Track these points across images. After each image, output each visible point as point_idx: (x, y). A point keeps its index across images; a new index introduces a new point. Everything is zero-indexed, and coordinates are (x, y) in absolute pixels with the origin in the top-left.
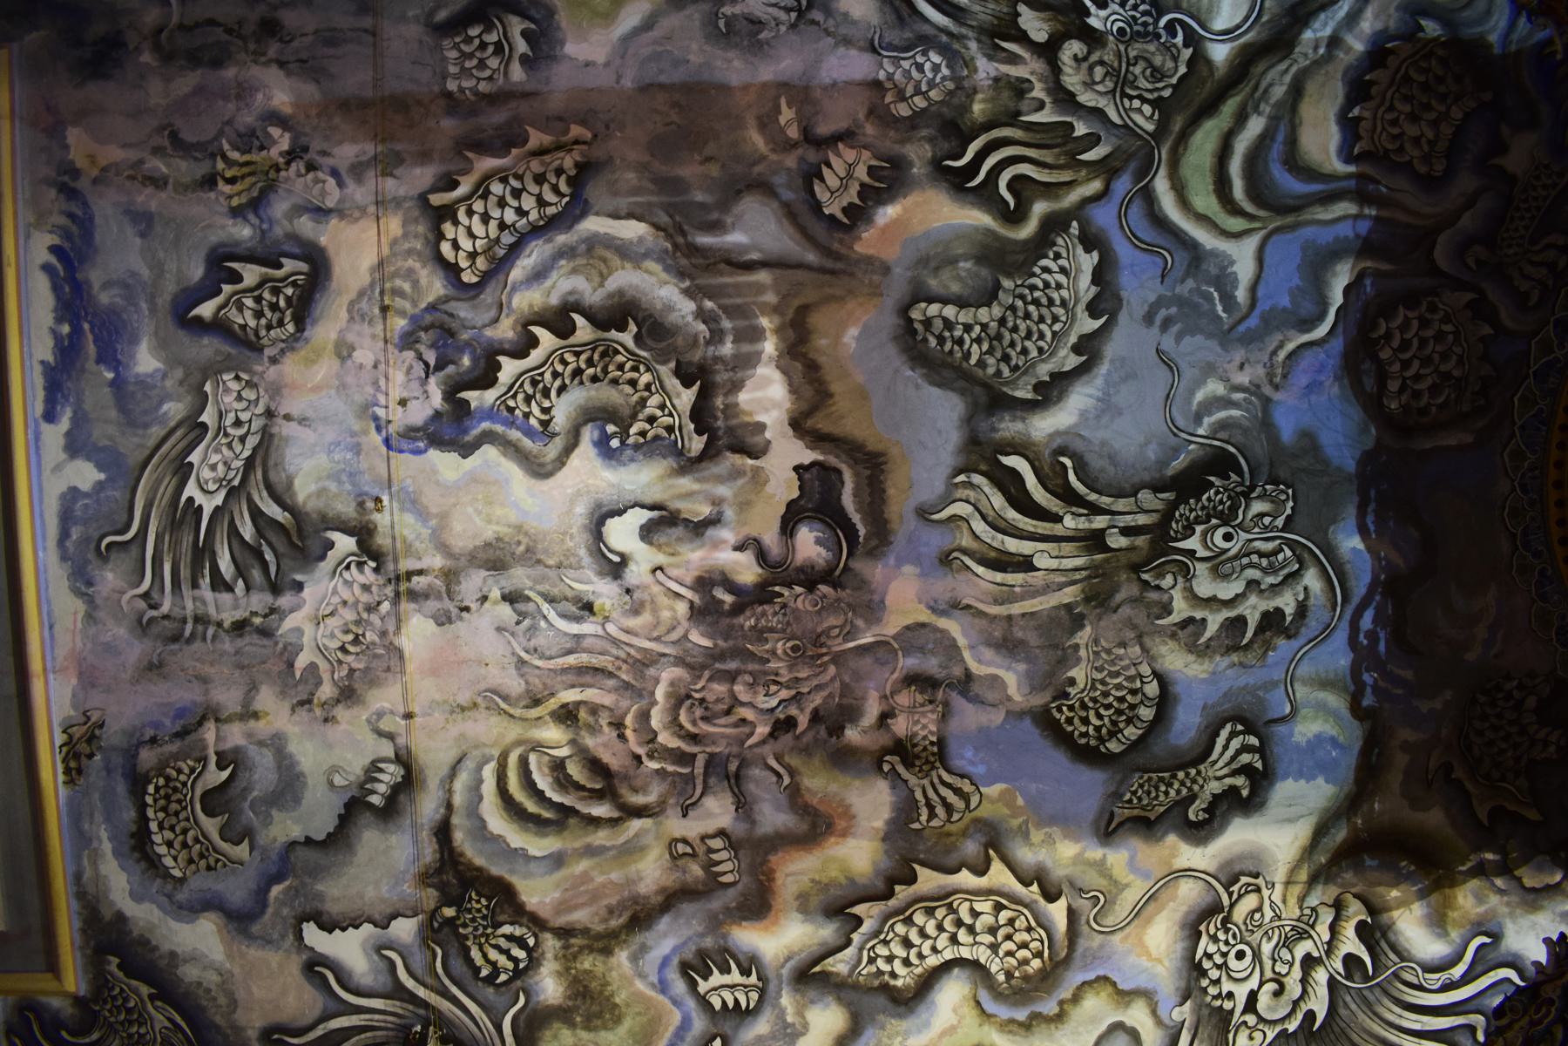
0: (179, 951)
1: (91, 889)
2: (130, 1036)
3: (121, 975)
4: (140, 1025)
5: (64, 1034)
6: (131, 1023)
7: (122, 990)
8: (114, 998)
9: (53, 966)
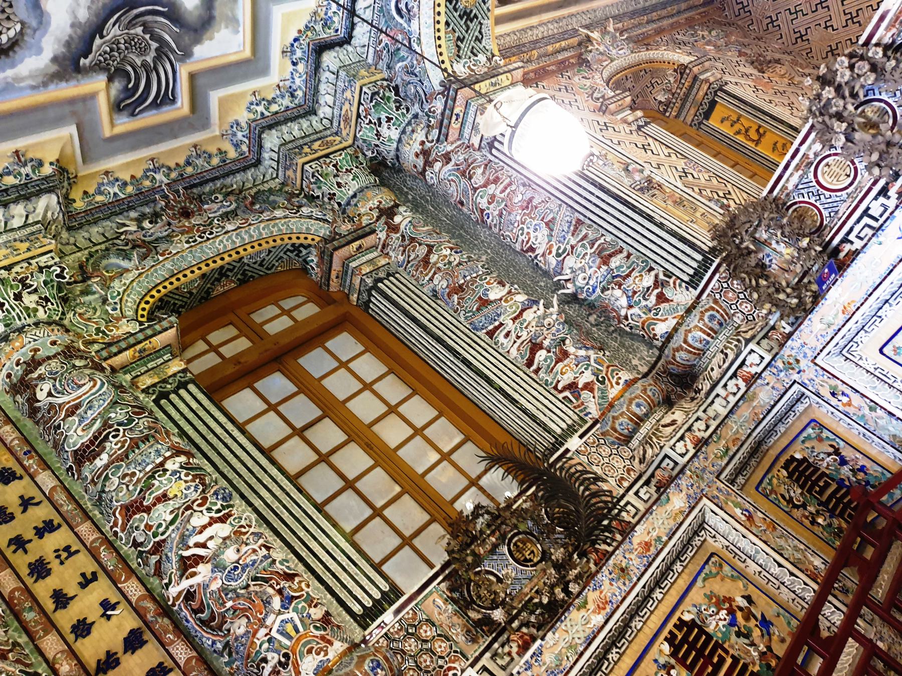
0: (69, 22)
1: (40, 79)
2: (127, 48)
3: (91, 57)
4: (119, 43)
5: (130, 86)
6: (119, 49)
7: (100, 55)
8: (105, 59)
9: (93, 96)
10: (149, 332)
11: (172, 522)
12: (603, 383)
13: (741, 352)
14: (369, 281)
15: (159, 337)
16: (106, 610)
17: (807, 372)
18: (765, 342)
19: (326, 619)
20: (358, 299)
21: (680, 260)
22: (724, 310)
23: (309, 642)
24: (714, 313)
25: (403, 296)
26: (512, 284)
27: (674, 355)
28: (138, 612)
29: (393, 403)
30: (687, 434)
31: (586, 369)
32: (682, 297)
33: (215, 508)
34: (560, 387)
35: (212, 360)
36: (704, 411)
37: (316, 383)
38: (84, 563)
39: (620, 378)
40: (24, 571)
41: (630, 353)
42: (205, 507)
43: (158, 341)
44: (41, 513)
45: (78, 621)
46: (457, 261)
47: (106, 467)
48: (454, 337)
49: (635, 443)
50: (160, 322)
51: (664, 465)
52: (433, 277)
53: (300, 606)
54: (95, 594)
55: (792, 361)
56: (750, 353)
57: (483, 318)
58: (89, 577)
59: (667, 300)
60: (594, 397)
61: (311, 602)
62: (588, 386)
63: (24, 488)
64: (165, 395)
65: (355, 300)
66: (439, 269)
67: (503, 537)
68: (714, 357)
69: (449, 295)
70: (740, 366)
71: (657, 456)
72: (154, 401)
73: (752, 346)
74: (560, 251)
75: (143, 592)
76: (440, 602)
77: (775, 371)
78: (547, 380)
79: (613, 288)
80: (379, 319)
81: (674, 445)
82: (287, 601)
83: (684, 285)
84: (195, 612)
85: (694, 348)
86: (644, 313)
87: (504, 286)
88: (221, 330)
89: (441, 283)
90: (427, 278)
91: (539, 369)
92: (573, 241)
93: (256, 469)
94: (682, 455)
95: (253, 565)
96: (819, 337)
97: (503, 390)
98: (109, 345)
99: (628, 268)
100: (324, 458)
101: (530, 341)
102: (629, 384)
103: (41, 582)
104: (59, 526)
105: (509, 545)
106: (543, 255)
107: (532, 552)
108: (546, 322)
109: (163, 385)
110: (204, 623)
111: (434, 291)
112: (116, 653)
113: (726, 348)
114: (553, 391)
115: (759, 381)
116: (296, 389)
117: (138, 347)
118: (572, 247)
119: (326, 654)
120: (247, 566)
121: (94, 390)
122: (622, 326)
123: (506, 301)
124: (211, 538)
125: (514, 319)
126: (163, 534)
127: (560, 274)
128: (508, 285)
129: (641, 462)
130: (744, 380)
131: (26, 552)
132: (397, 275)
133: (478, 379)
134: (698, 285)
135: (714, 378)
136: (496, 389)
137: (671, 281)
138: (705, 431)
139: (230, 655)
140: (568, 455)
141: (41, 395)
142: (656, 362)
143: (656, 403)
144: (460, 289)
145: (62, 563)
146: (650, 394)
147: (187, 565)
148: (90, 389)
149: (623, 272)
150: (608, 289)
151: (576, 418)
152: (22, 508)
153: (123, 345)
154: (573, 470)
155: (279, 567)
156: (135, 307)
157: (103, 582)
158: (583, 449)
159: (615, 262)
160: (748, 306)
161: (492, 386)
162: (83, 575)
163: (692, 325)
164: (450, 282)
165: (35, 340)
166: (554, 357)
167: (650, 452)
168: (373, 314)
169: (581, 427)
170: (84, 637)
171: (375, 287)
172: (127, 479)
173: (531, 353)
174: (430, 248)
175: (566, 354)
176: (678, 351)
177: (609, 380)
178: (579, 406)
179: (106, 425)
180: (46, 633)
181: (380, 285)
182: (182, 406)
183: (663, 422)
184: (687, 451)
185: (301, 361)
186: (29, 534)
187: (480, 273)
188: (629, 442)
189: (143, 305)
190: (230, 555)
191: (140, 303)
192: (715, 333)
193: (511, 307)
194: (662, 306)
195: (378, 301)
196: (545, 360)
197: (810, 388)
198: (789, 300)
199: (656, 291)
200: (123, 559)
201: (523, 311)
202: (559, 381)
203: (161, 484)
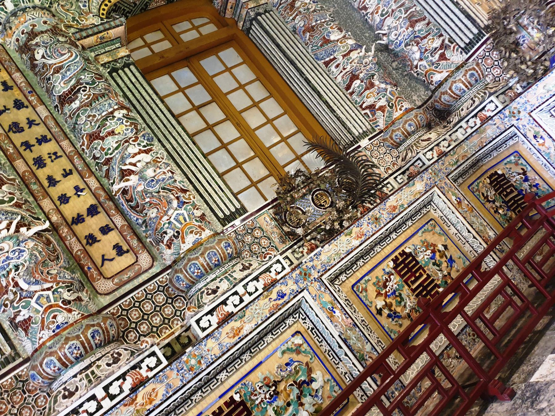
10: (107, 26)
11: (117, 148)
12: (391, 107)
13: (485, 101)
14: (252, 14)
15: (114, 30)
16: (77, 191)
17: (523, 120)
18: (501, 97)
19: (203, 217)
20: (243, 26)
21: (462, 32)
22: (481, 71)
23: (191, 227)
24: (474, 72)
25: (273, 28)
26: (347, 31)
27: (441, 97)
29: (257, 100)
30: (436, 148)
31: (383, 97)
32: (457, 58)
33: (142, 144)
34: (363, 107)
35: (146, 52)
36: (450, 135)
37: (210, 78)
38: (64, 163)
39: (403, 106)
40: (31, 162)
41: (413, 91)
42: (136, 143)
43: (113, 33)
44: (39, 131)
45: (62, 194)
46: (313, 9)
47: (78, 109)
48: (302, 62)
49: (402, 148)
50: (114, 20)
51: (416, 164)
52: (295, 17)
53: (188, 208)
54: (71, 182)
55: (515, 111)
56: (490, 102)
57: (324, 52)
58: (68, 172)
59: (446, 59)
60: (384, 116)
61: (195, 207)
62: (382, 109)
63: (29, 113)
64: (115, 70)
65: (241, 26)
66: (300, 12)
67: (310, 190)
68: (465, 102)
69: (304, 32)
70: (481, 110)
71: (414, 158)
72: (108, 72)
73: (492, 98)
74: (384, 13)
75: (98, 185)
76: (268, 219)
77: (502, 116)
78: (356, 101)
79: (413, 45)
80: (255, 42)
81: (426, 153)
82: (182, 204)
83: (460, 49)
84: (128, 201)
85: (455, 94)
86: (429, 65)
87: (341, 31)
88: (153, 33)
89: (300, 23)
90: (291, 18)
91: (353, 93)
92: (394, 7)
93: (169, 126)
94: (429, 160)
95: (163, 180)
96: (539, 98)
97: (328, 103)
98: (81, 30)
99: (426, 32)
100: (210, 127)
101: (352, 72)
102: (408, 111)
103: (40, 169)
104: (50, 140)
105: (313, 195)
106: (372, 13)
107: (326, 201)
108: (364, 61)
109: (115, 63)
110: (132, 207)
111: (294, 27)
112: (83, 215)
113: (475, 97)
114: (359, 108)
115: (490, 122)
116: (197, 81)
117: (100, 35)
118: (393, 11)
119: (201, 235)
120: (160, 181)
121: (71, 59)
122: (413, 72)
123: (341, 42)
124: (139, 161)
125: (344, 56)
126: (111, 154)
127: (381, 29)
128: (344, 32)
129: (402, 160)
130: (481, 120)
131: (31, 151)
132: (271, 13)
133: (313, 93)
134: (469, 51)
135: (462, 115)
136: (323, 101)
137: (452, 46)
138: (447, 147)
139: (146, 227)
140: (359, 150)
141: (38, 56)
142: (428, 100)
143: (421, 125)
144: (311, 29)
145: (52, 161)
146: (419, 119)
147: (124, 174)
148: (69, 58)
149: (422, 34)
150: (410, 45)
151: (369, 127)
152: (28, 126)
153: (90, 32)
154: (360, 159)
155: (178, 184)
156: (98, 7)
157: (75, 175)
158: (369, 147)
159: (419, 26)
160: (499, 71)
161: (321, 99)
162: (64, 170)
163: (457, 79)
164: (306, 23)
165: (33, 19)
166: (364, 86)
167: (410, 155)
168: (252, 38)
169: (372, 133)
170: (65, 204)
171: (255, 19)
172: (91, 118)
173: (350, 81)
175: (372, 85)
176: (444, 94)
177: (396, 106)
178: (373, 120)
179: (78, 82)
180: (44, 198)
181: (259, 17)
182: (126, 79)
183: (422, 138)
184: (433, 158)
185: (202, 62)
186: (33, 142)
187: (327, 20)
188: (399, 147)
189: (103, 7)
190: (150, 173)
191: (101, 4)
192: (471, 86)
193: (343, 47)
194: (441, 62)
195: (256, 29)
196: (358, 87)
197: (522, 131)
198: (527, 70)
199: (441, 51)
200: (87, 165)
201: (351, 51)
202: (364, 103)
203: (111, 125)
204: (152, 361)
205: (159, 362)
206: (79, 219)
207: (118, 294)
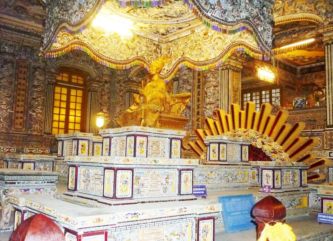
14: (92, 90)
28: (24, 110)
38: (23, 98)
61: (41, 127)
100: (60, 108)
141: (36, 73)
147: (34, 111)
174: (105, 94)
179: (39, 85)
186: (21, 89)
195: (90, 93)
204: (13, 150)
205: (14, 151)
206: (18, 112)
207: (14, 132)
